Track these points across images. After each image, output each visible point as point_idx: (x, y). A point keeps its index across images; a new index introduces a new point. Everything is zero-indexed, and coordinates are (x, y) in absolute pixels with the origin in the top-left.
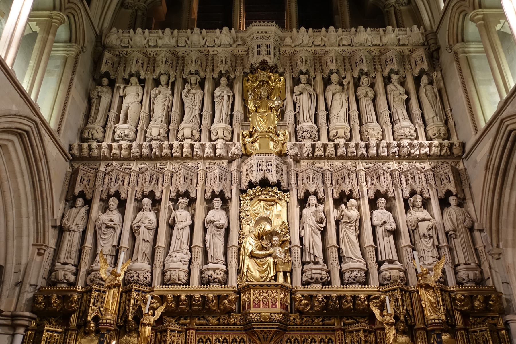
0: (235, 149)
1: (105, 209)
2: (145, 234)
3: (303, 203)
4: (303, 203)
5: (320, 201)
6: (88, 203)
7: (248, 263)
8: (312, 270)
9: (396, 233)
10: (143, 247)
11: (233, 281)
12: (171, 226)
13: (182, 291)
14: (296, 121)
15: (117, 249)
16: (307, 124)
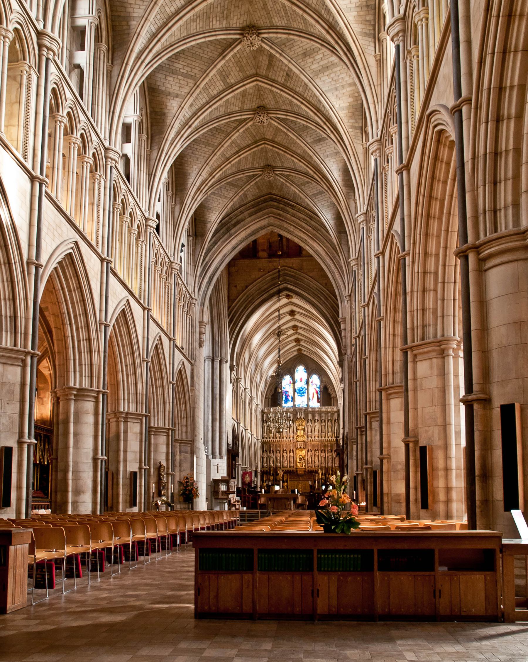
0: (295, 440)
1: (270, 452)
2: (279, 458)
3: (308, 451)
4: (308, 451)
5: (311, 451)
6: (266, 451)
7: (298, 464)
8: (310, 465)
9: (325, 458)
10: (279, 461)
11: (295, 467)
12: (283, 456)
13: (287, 469)
14: (308, 432)
15: (273, 461)
16: (310, 434)
